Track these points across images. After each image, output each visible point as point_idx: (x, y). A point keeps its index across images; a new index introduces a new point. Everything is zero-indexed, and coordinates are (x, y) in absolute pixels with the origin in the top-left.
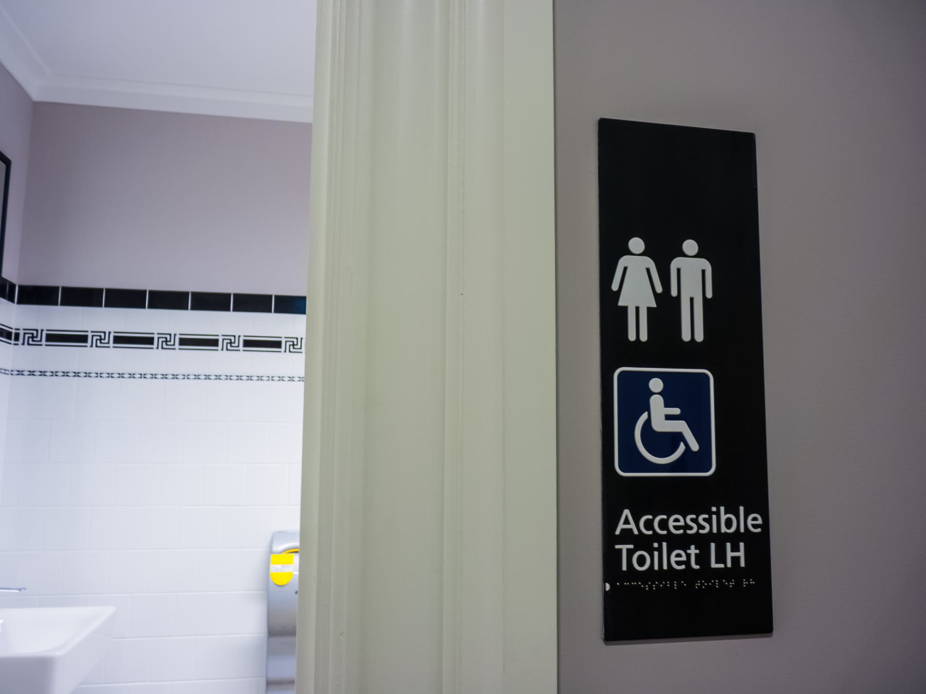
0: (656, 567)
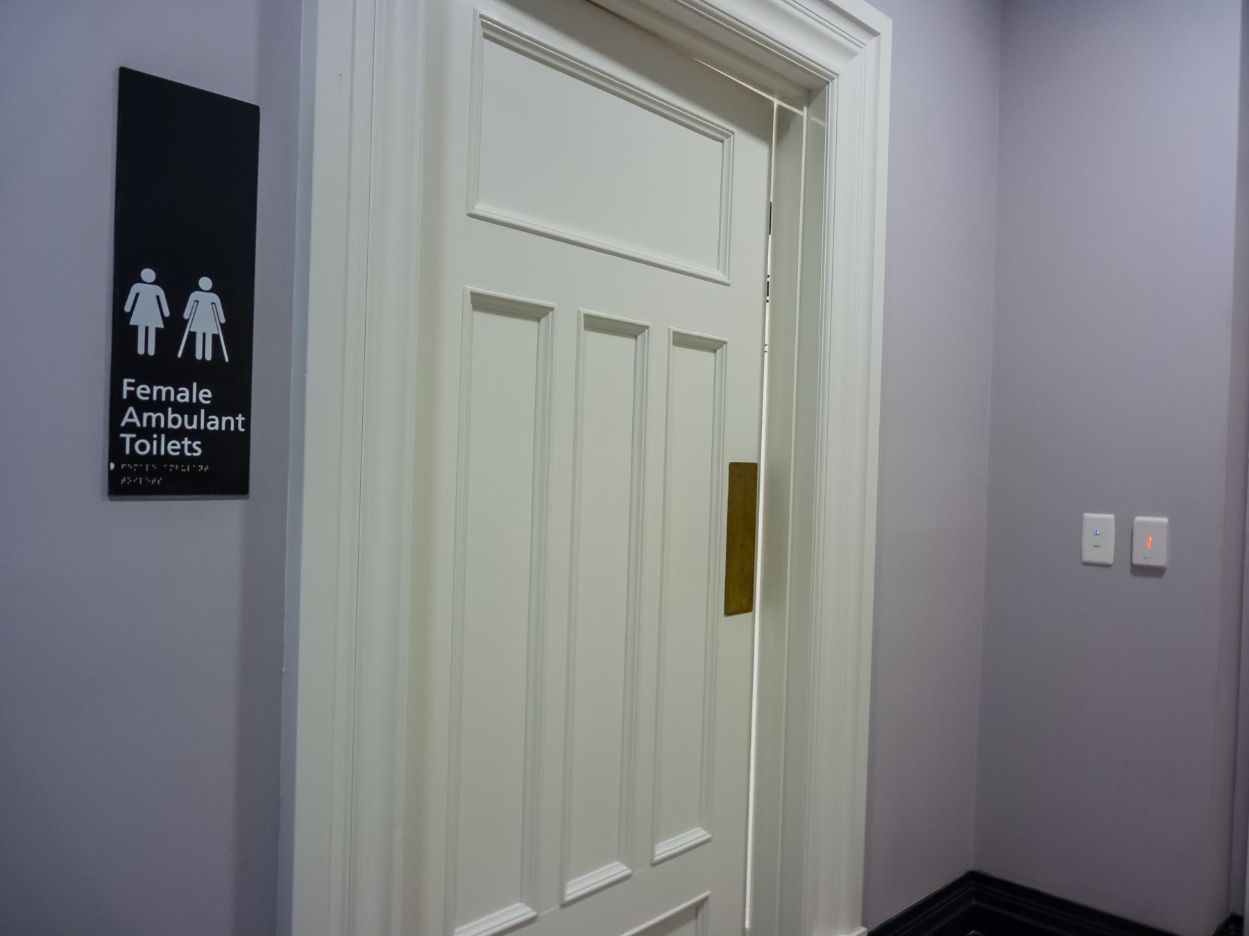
0: (155, 452)
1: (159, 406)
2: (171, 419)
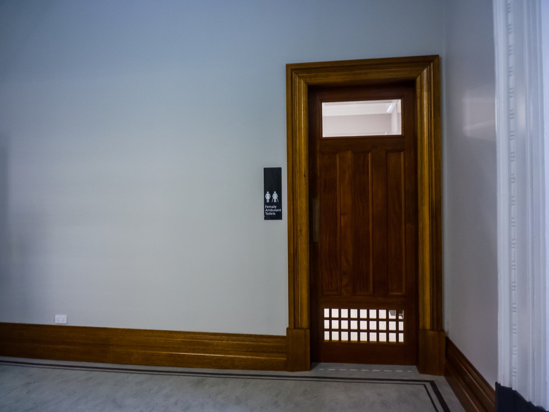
1: (270, 209)
2: (271, 210)
